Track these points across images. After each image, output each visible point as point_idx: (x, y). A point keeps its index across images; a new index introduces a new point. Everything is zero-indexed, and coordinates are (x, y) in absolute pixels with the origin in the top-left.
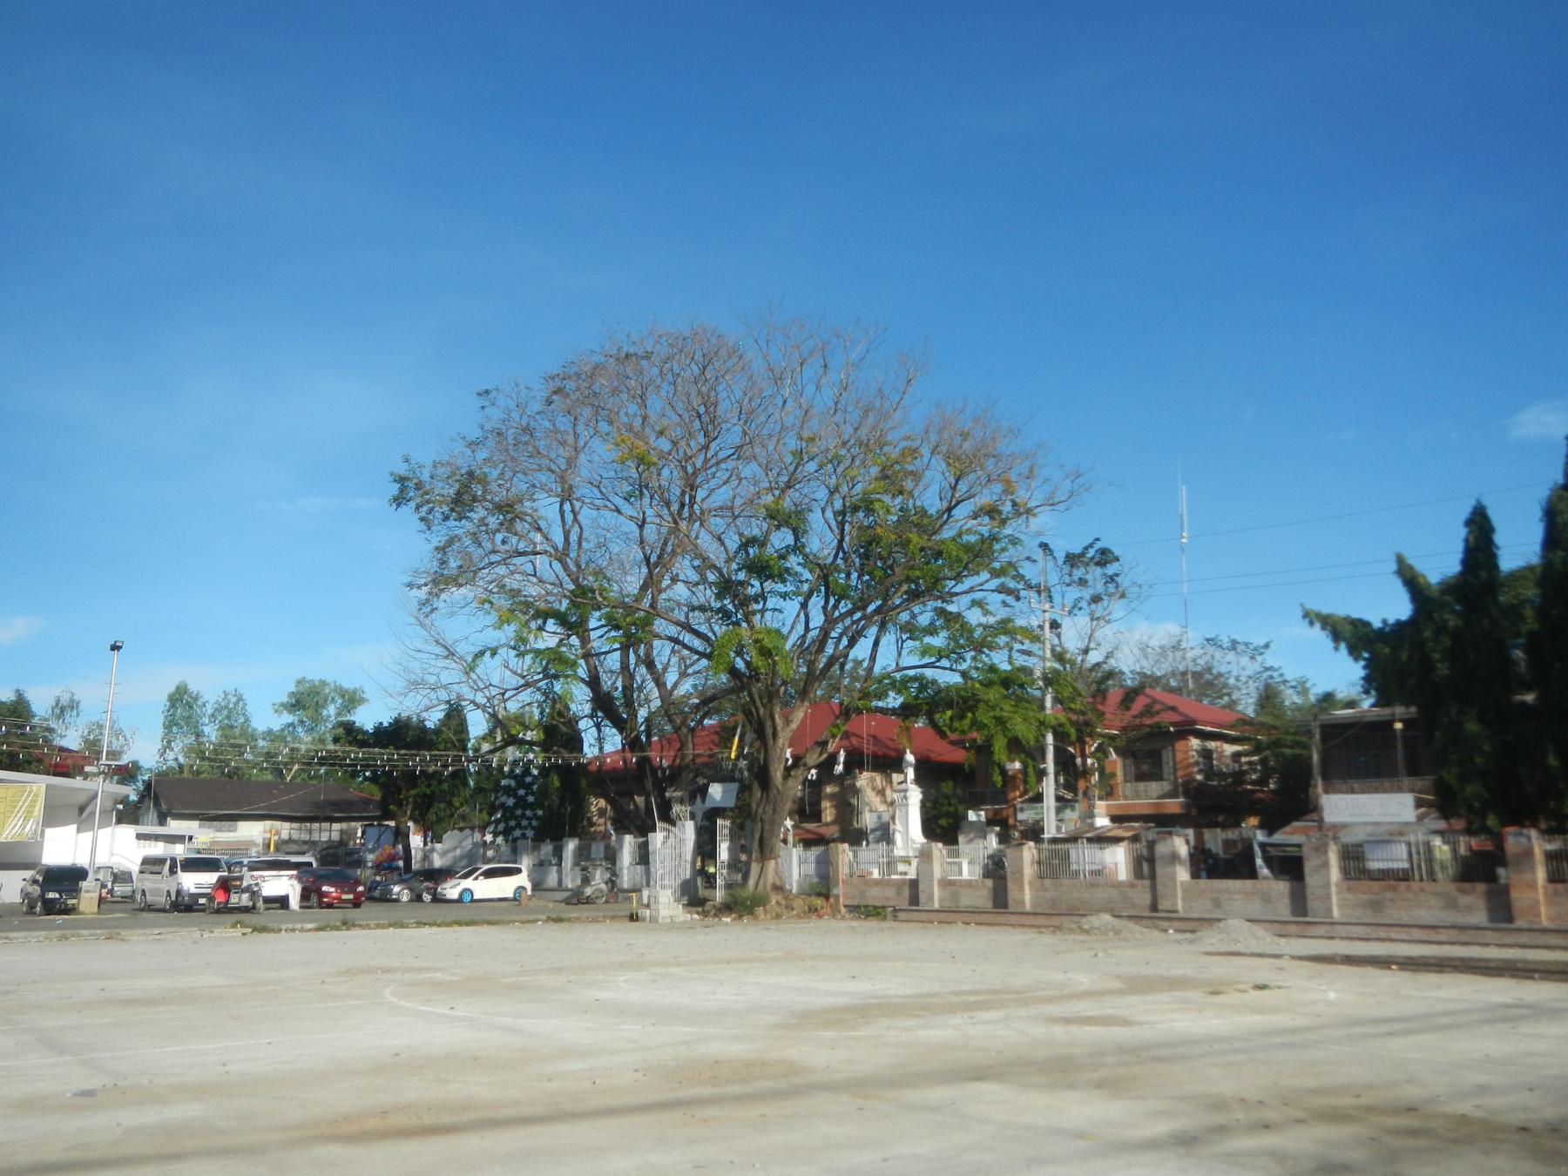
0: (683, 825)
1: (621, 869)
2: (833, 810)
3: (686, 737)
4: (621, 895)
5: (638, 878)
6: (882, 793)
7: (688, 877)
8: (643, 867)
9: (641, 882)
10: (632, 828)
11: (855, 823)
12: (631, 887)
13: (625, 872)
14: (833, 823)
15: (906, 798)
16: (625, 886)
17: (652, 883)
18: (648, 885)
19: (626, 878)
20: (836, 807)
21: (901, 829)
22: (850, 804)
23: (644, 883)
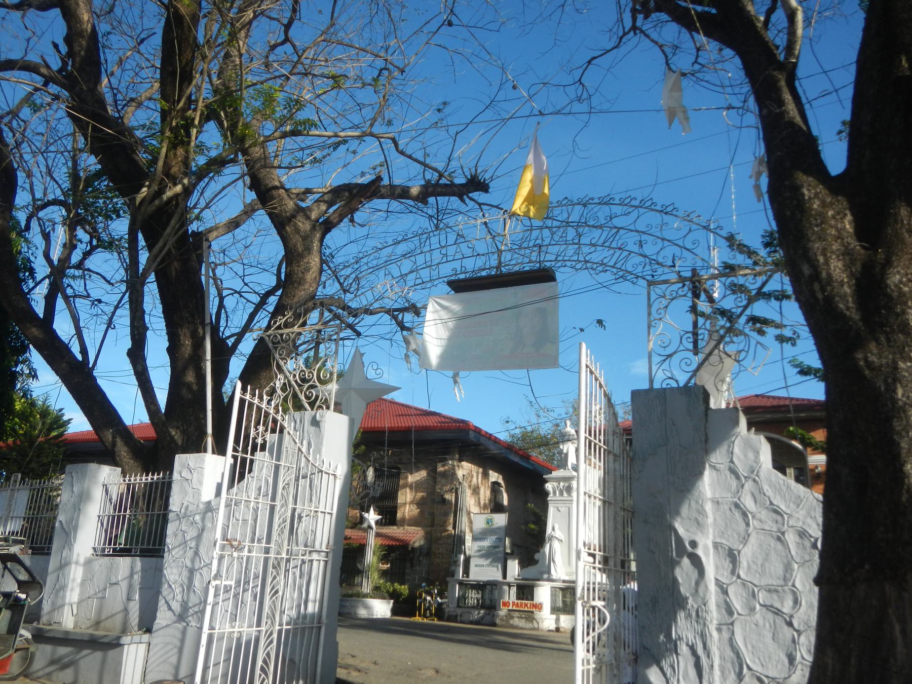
0: (315, 423)
1: (64, 566)
2: (414, 507)
3: (306, 238)
4: (44, 652)
5: (116, 598)
6: (476, 491)
7: (312, 608)
8: (138, 562)
9: (126, 610)
10: (122, 451)
11: (450, 528)
12: (85, 629)
13: (76, 574)
14: (414, 522)
15: (569, 489)
16: (68, 621)
17: (163, 617)
18: (147, 626)
19: (73, 595)
20: (420, 504)
21: (562, 537)
22: (444, 501)
23: (134, 618)
